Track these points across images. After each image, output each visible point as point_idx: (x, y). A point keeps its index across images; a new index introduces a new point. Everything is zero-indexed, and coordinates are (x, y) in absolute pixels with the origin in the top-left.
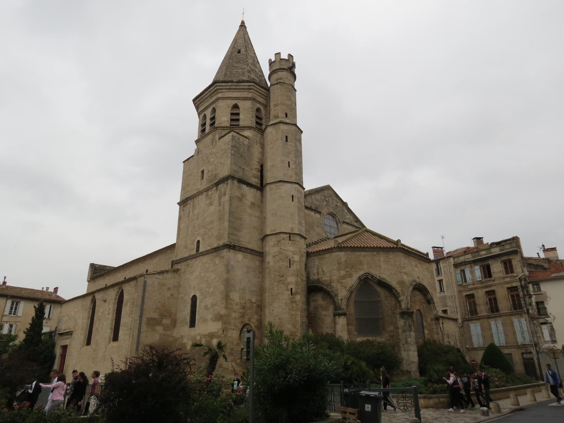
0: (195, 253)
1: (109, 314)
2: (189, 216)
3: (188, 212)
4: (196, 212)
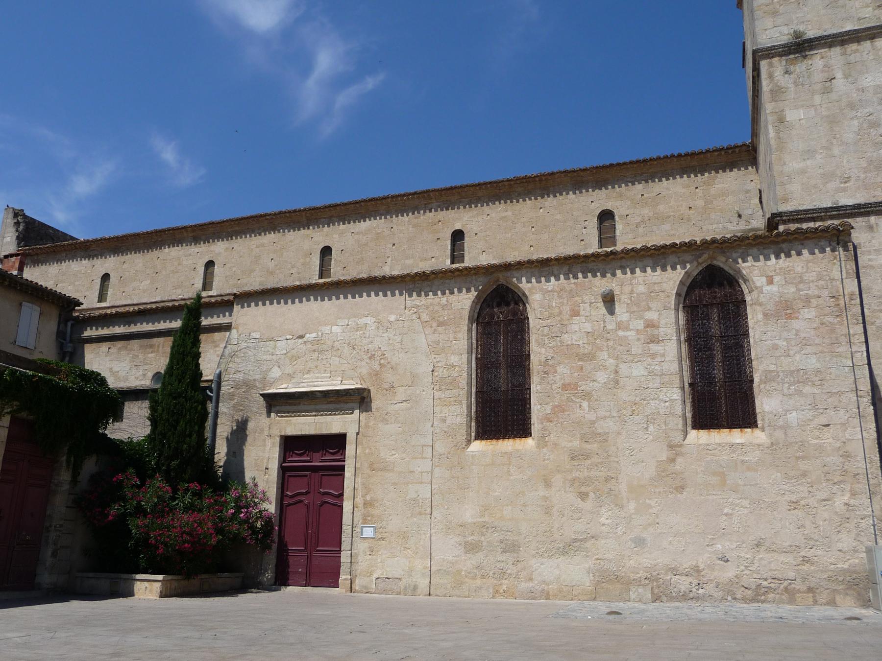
1: (655, 340)
2: (827, 91)
3: (818, 77)
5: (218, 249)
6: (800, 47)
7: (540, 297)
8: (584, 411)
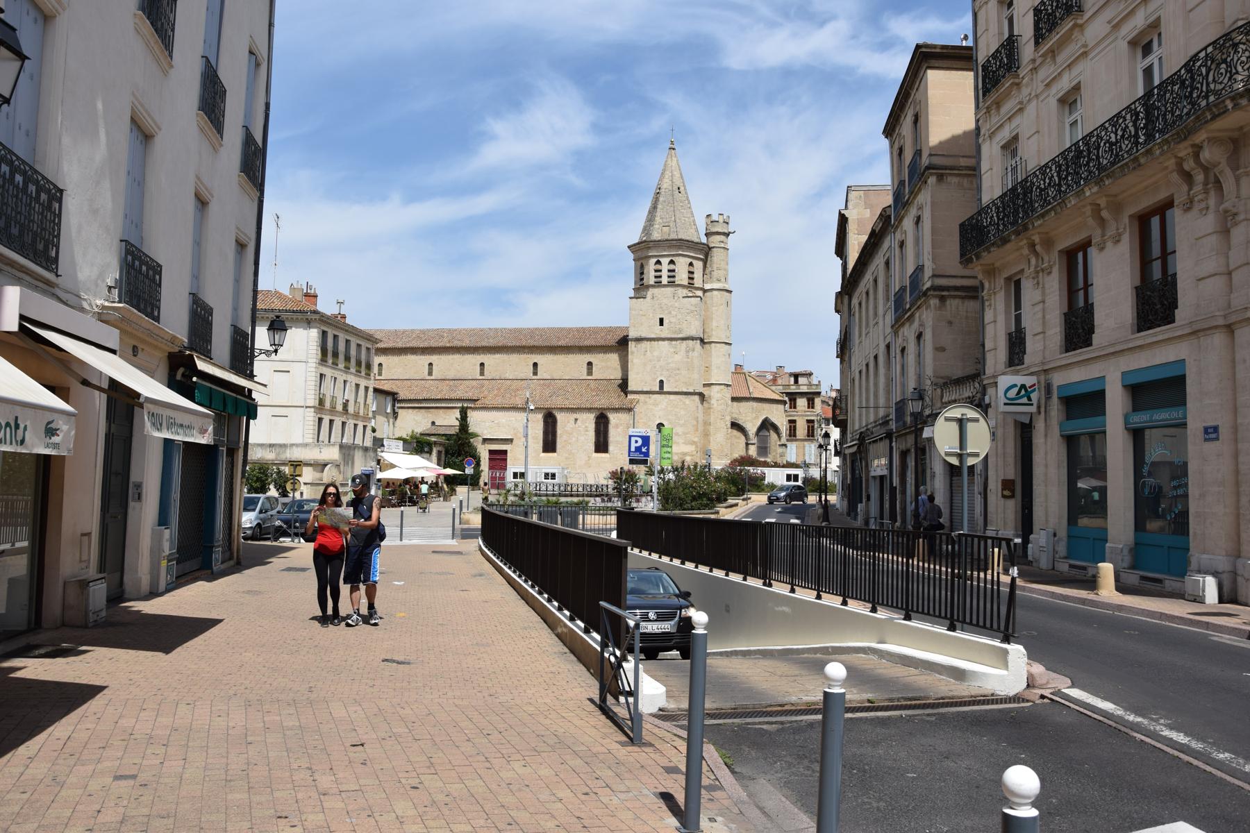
0: (657, 389)
4: (656, 354)
5: (434, 358)
6: (639, 340)
7: (560, 417)
8: (569, 447)
